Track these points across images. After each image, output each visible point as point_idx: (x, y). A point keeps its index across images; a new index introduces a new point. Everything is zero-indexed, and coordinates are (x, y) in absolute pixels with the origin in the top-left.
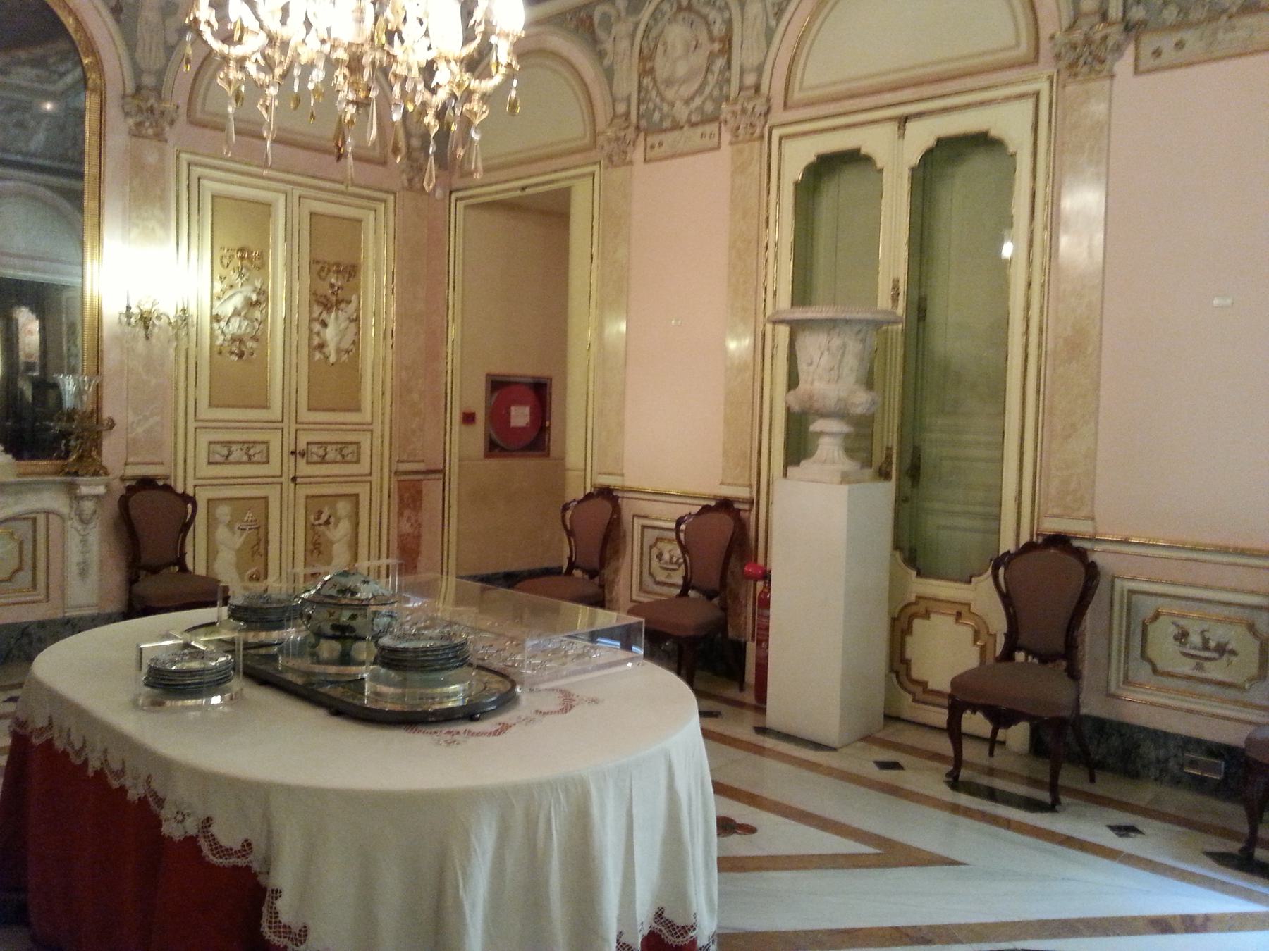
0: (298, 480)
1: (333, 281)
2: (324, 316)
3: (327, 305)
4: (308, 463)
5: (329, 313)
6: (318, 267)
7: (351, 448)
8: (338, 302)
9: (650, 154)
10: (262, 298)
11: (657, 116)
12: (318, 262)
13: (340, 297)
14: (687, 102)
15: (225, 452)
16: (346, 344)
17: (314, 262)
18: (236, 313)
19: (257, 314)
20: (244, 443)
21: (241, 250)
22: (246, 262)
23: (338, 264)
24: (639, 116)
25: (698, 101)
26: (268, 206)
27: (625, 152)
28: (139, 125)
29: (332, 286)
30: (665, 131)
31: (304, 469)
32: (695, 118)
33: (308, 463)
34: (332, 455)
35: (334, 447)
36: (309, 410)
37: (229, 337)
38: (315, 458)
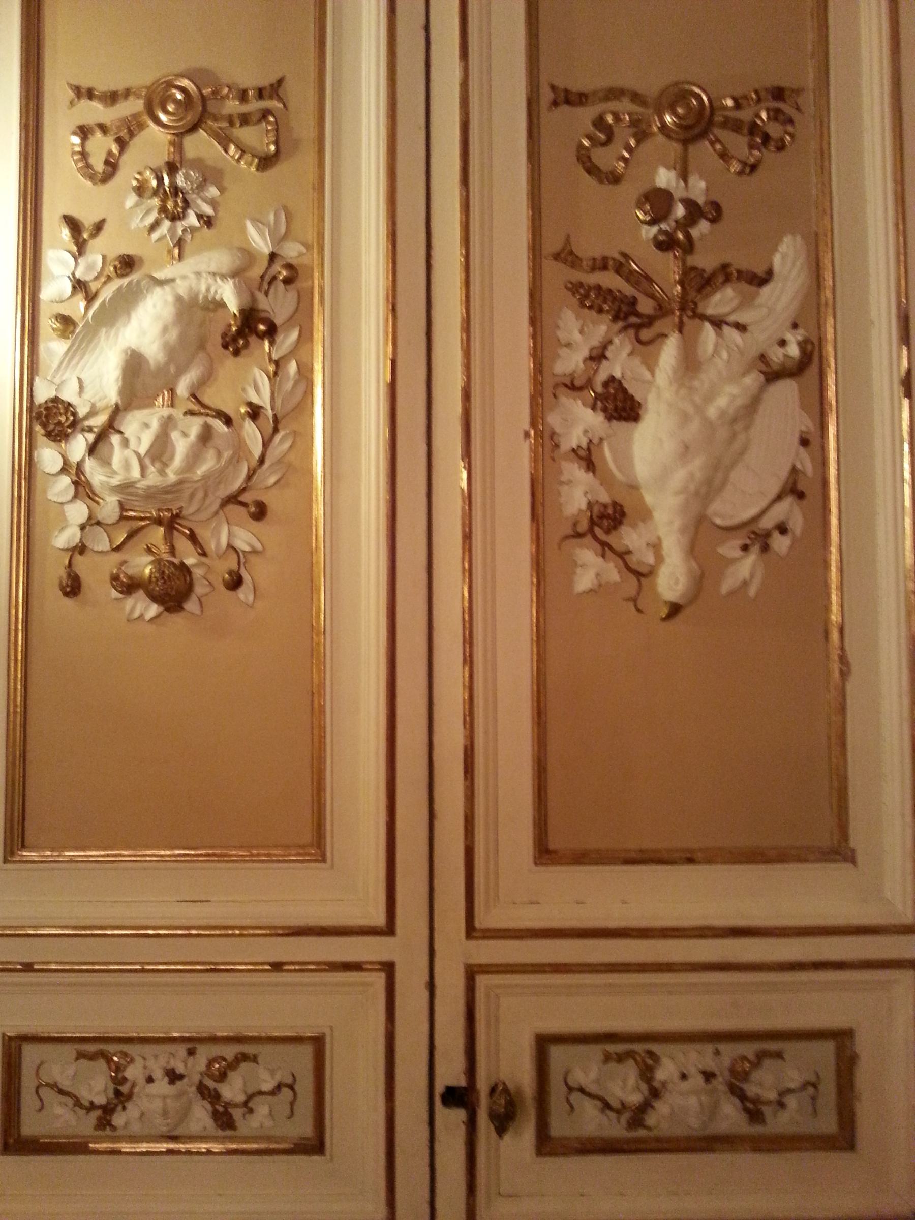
1: (665, 178)
2: (621, 363)
3: (634, 316)
4: (546, 1145)
5: (646, 346)
8: (701, 283)
10: (278, 305)
12: (570, 98)
13: (705, 261)
15: (96, 1086)
16: (748, 495)
17: (549, 98)
18: (140, 381)
20: (192, 1044)
29: (658, 202)
33: (546, 1145)
34: (683, 1105)
35: (697, 1058)
36: (545, 853)
37: (109, 508)
38: (591, 1121)
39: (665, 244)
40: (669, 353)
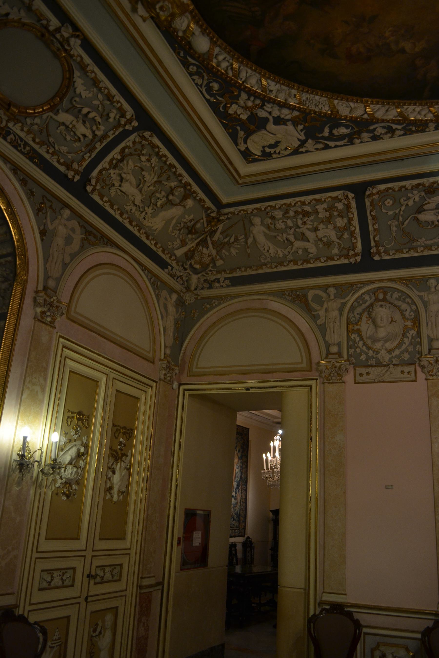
0: (90, 599)
1: (121, 440)
6: (115, 428)
7: (118, 568)
9: (358, 378)
11: (363, 357)
12: (115, 426)
13: (123, 452)
14: (390, 352)
17: (114, 425)
19: (81, 463)
21: (79, 413)
22: (80, 423)
23: (124, 428)
24: (349, 356)
25: (397, 352)
26: (97, 382)
27: (341, 376)
28: (43, 313)
29: (121, 443)
30: (371, 366)
31: (96, 590)
32: (394, 362)
37: (64, 480)
39: (120, 449)
40: (119, 465)
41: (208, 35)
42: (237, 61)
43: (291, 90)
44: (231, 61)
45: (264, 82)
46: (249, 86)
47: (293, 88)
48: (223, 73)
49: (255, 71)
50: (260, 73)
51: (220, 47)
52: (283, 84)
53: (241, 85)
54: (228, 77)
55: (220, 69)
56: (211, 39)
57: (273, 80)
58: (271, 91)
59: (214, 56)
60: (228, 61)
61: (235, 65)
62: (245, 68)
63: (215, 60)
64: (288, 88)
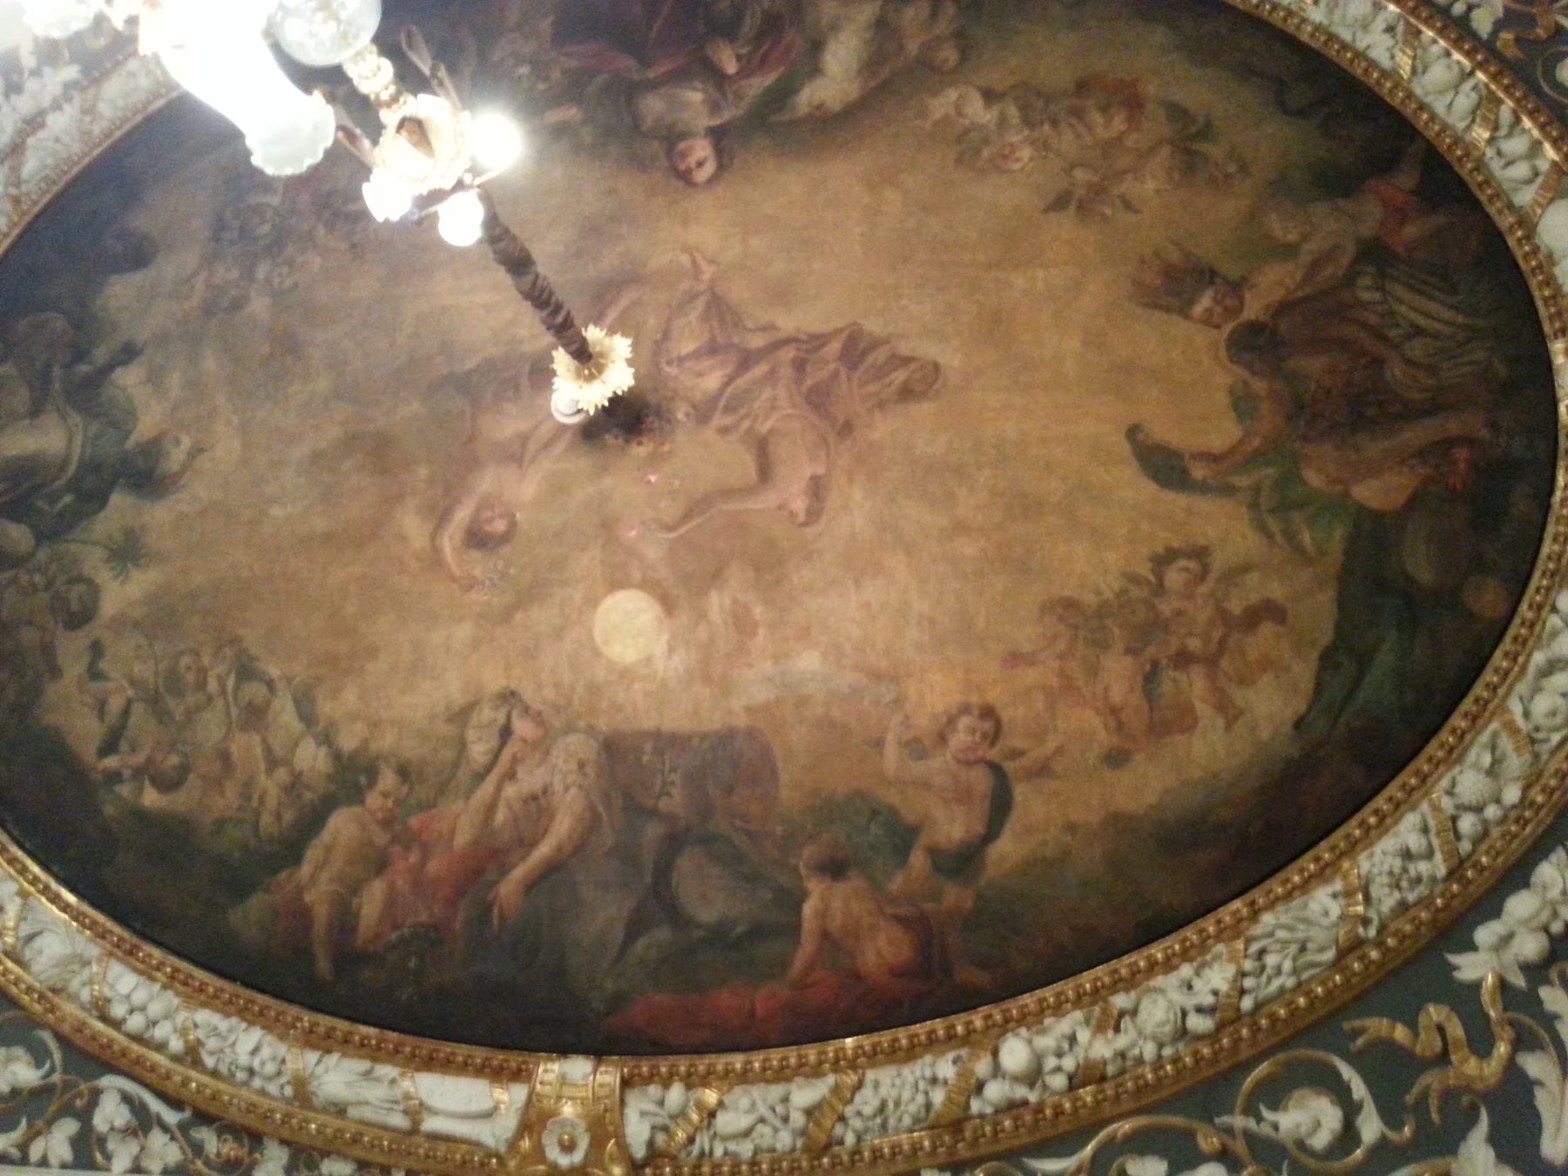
41: (1536, 250)
42: (1469, 149)
43: (1326, 22)
44: (1490, 152)
45: (1405, 63)
46: (1457, 56)
47: (1318, 28)
48: (1532, 114)
49: (1422, 107)
50: (1410, 95)
51: (1510, 206)
52: (1345, 47)
53: (1480, 66)
54: (1518, 101)
55: (1536, 133)
56: (1529, 237)
57: (1373, 64)
58: (1390, 29)
59: (1540, 180)
60: (1499, 153)
61: (1481, 134)
62: (1450, 120)
63: (1544, 166)
64: (1334, 29)
